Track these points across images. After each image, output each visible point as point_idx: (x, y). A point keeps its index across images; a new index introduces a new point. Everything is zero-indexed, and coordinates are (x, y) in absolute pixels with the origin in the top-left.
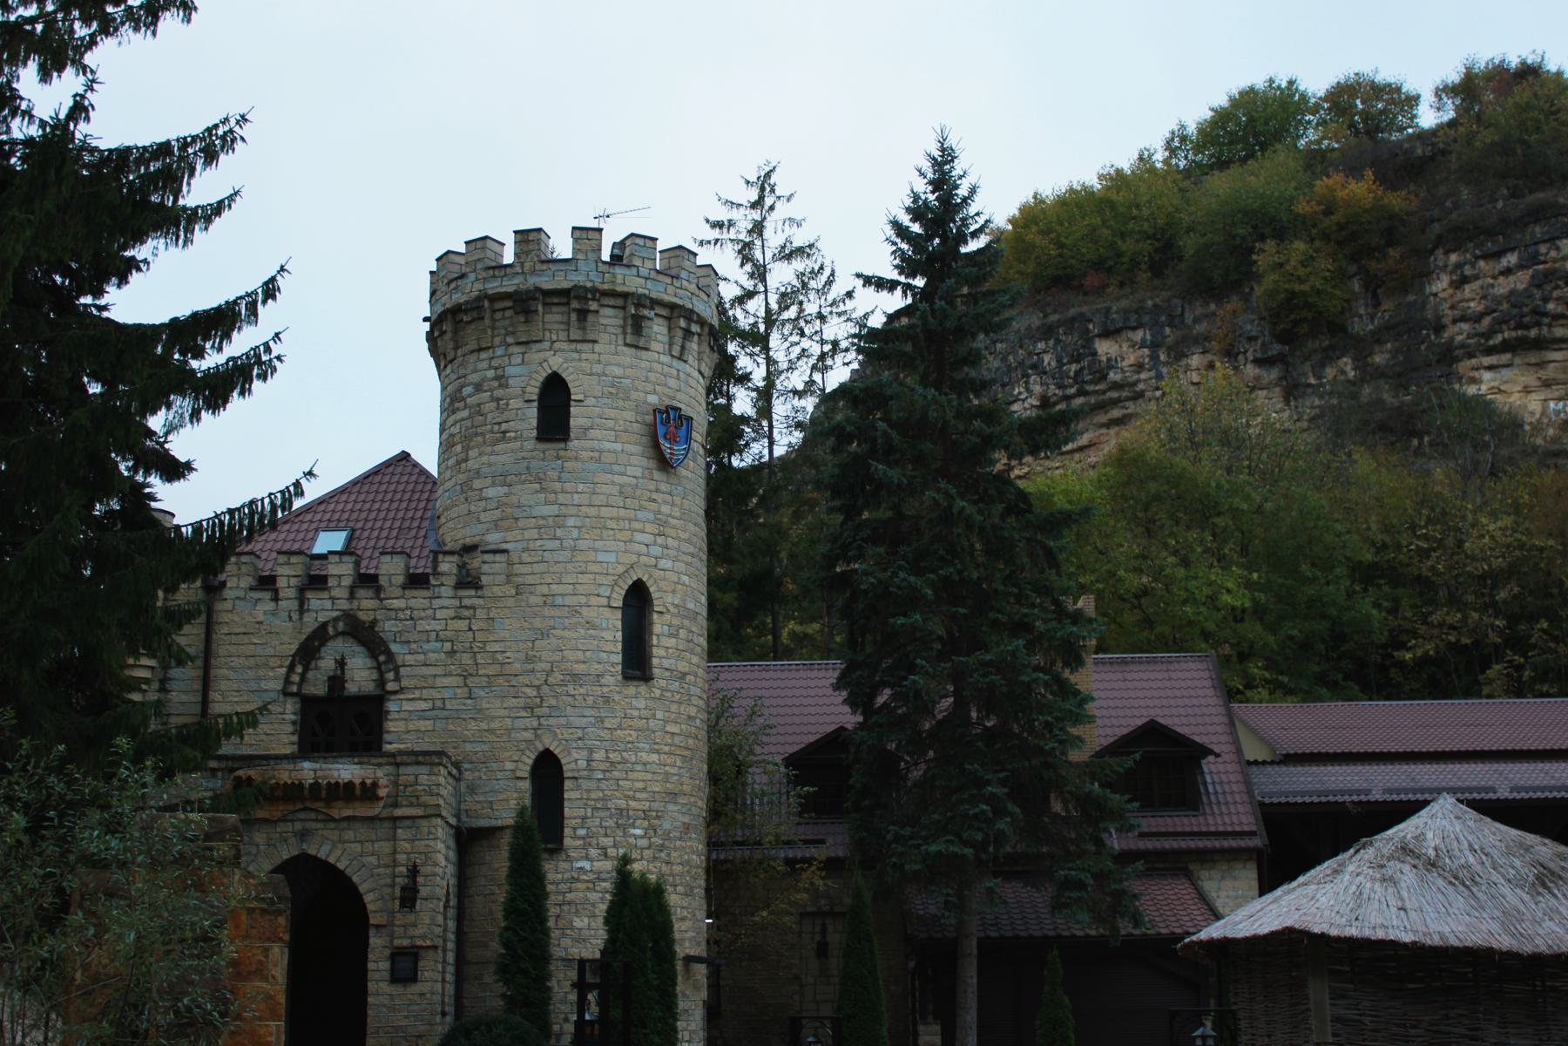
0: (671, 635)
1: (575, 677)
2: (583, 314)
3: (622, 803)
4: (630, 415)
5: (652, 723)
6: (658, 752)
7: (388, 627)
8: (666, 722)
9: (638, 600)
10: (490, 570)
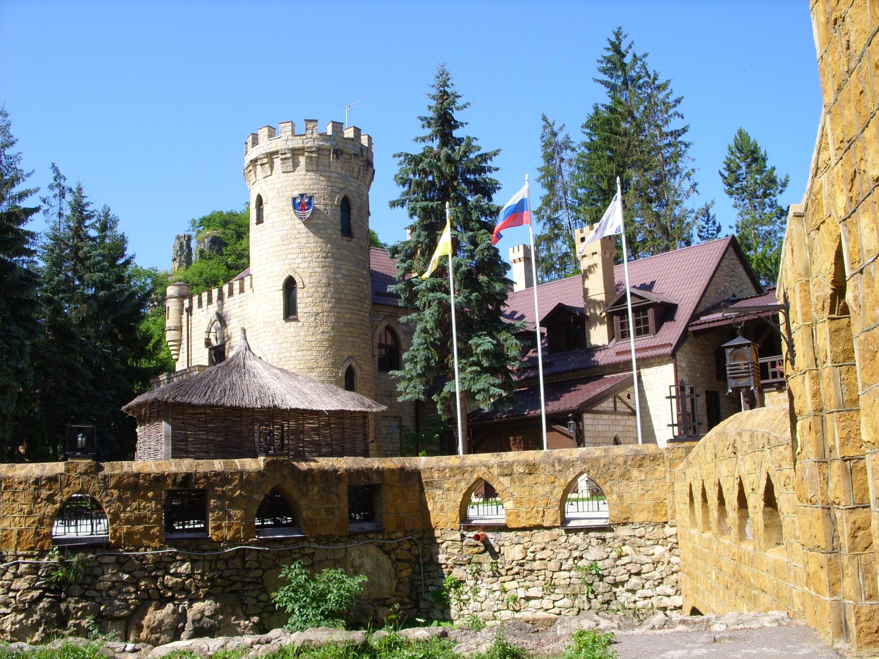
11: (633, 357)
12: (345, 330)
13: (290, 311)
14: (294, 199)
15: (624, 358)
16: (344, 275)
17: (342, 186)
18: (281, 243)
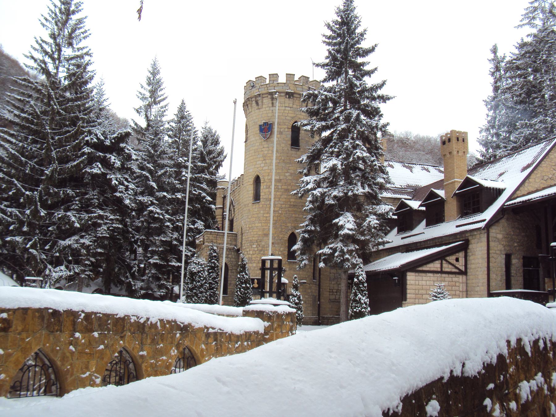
0: (266, 188)
3: (251, 239)
5: (259, 215)
6: (261, 223)
8: (264, 214)
12: (290, 209)
14: (260, 126)
16: (291, 174)
17: (293, 115)
18: (254, 154)
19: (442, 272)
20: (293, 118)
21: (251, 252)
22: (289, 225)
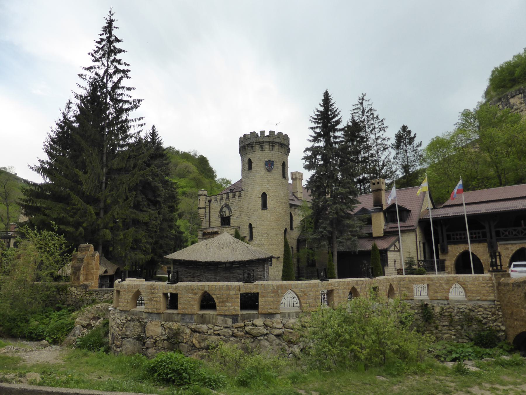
1: (254, 210)
2: (252, 147)
4: (261, 163)
7: (230, 205)
9: (264, 196)
10: (243, 193)
11: (399, 229)
13: (264, 206)
15: (396, 229)
19: (394, 251)
20: (283, 159)
21: (263, 240)
22: (284, 223)
